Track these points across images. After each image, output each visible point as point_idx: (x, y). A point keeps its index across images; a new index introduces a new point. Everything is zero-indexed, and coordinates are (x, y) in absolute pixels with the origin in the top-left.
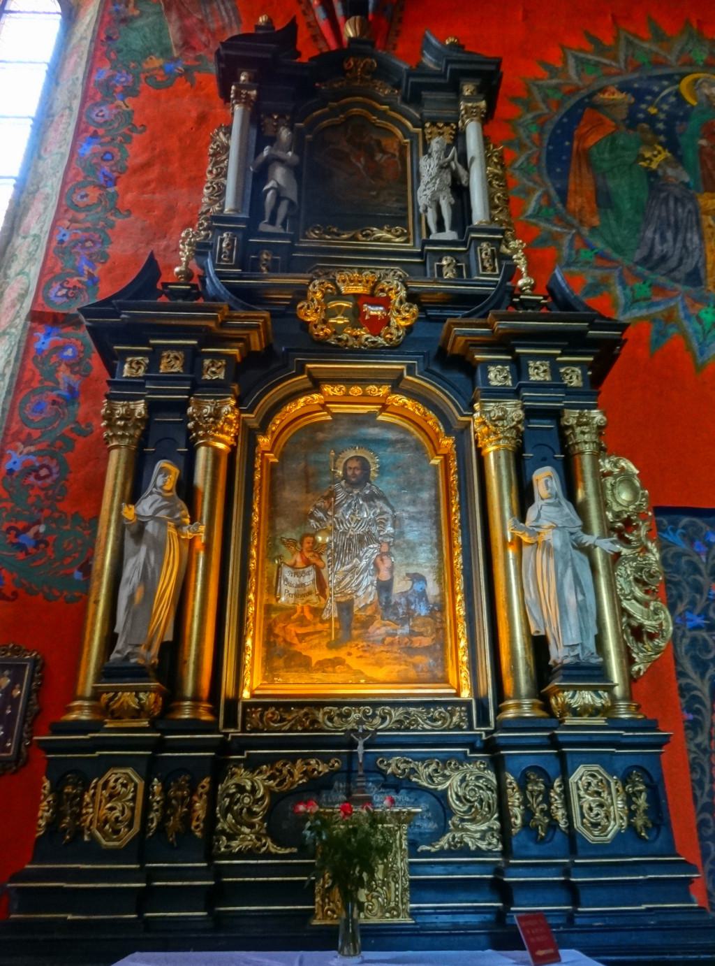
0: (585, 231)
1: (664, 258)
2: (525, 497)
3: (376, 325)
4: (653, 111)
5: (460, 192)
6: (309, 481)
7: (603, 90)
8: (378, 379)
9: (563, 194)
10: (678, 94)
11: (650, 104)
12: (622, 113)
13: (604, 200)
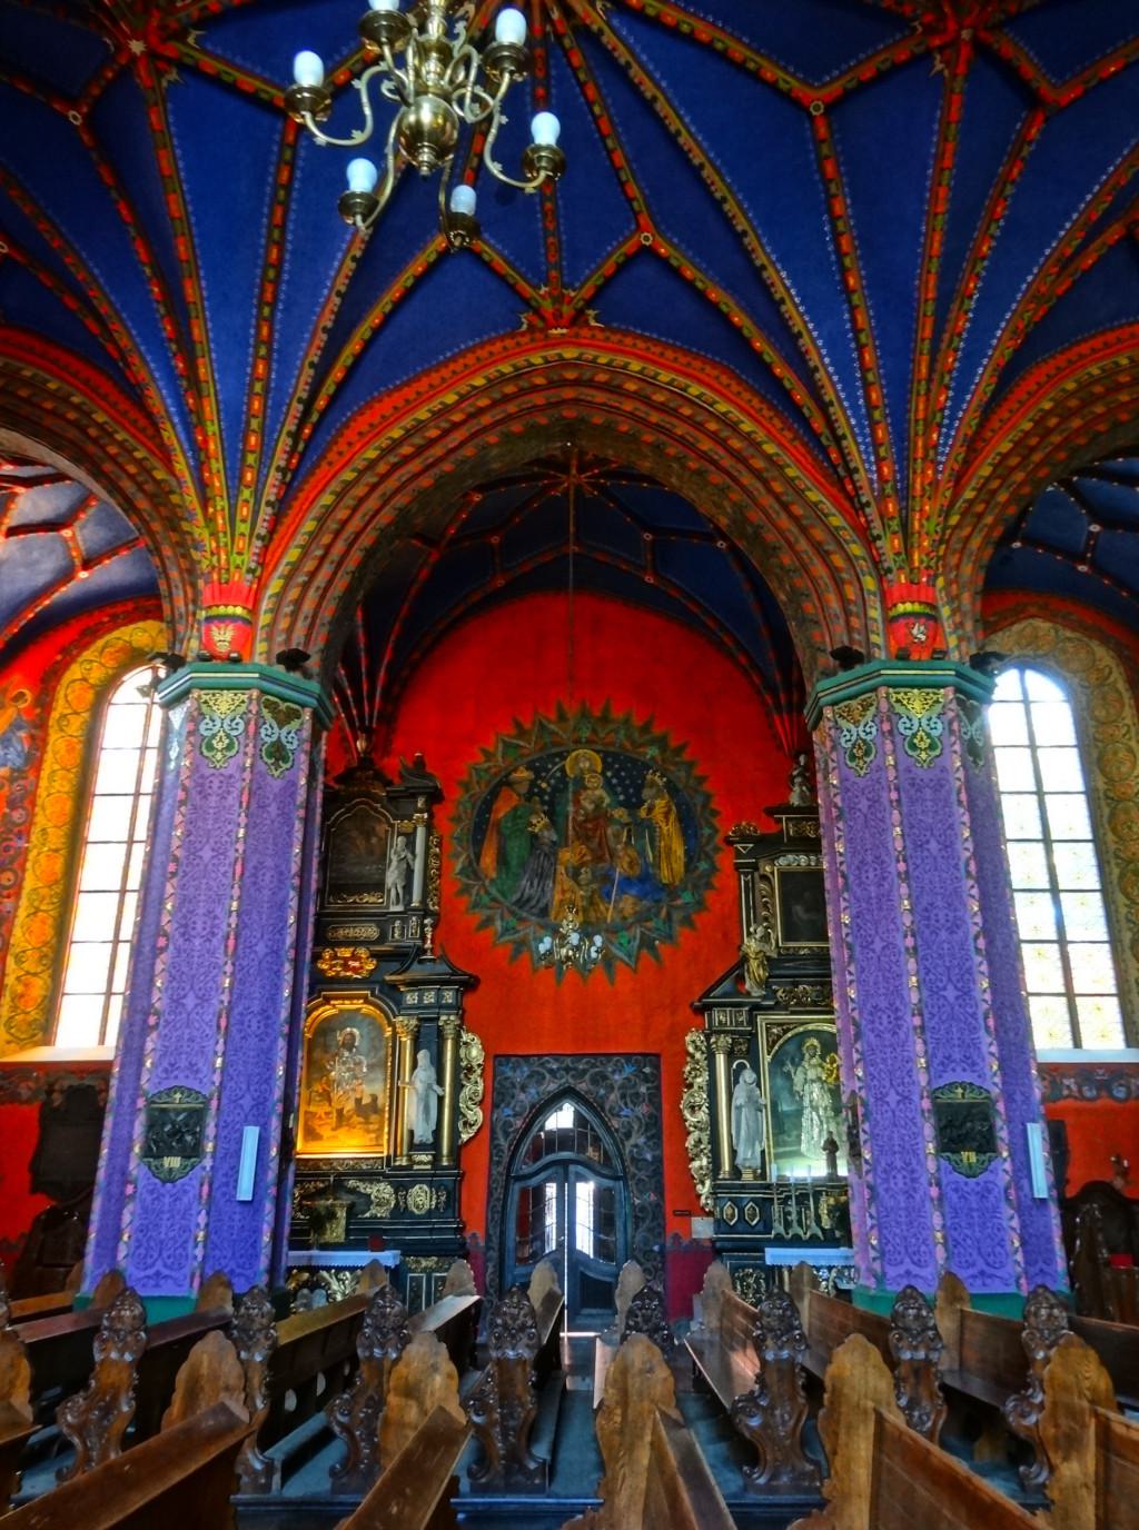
0: (487, 882)
1: (529, 900)
2: (414, 1065)
3: (355, 970)
4: (544, 785)
5: (409, 872)
6: (326, 1048)
7: (515, 770)
8: (358, 997)
9: (478, 857)
10: (563, 770)
11: (543, 779)
12: (523, 789)
13: (502, 860)
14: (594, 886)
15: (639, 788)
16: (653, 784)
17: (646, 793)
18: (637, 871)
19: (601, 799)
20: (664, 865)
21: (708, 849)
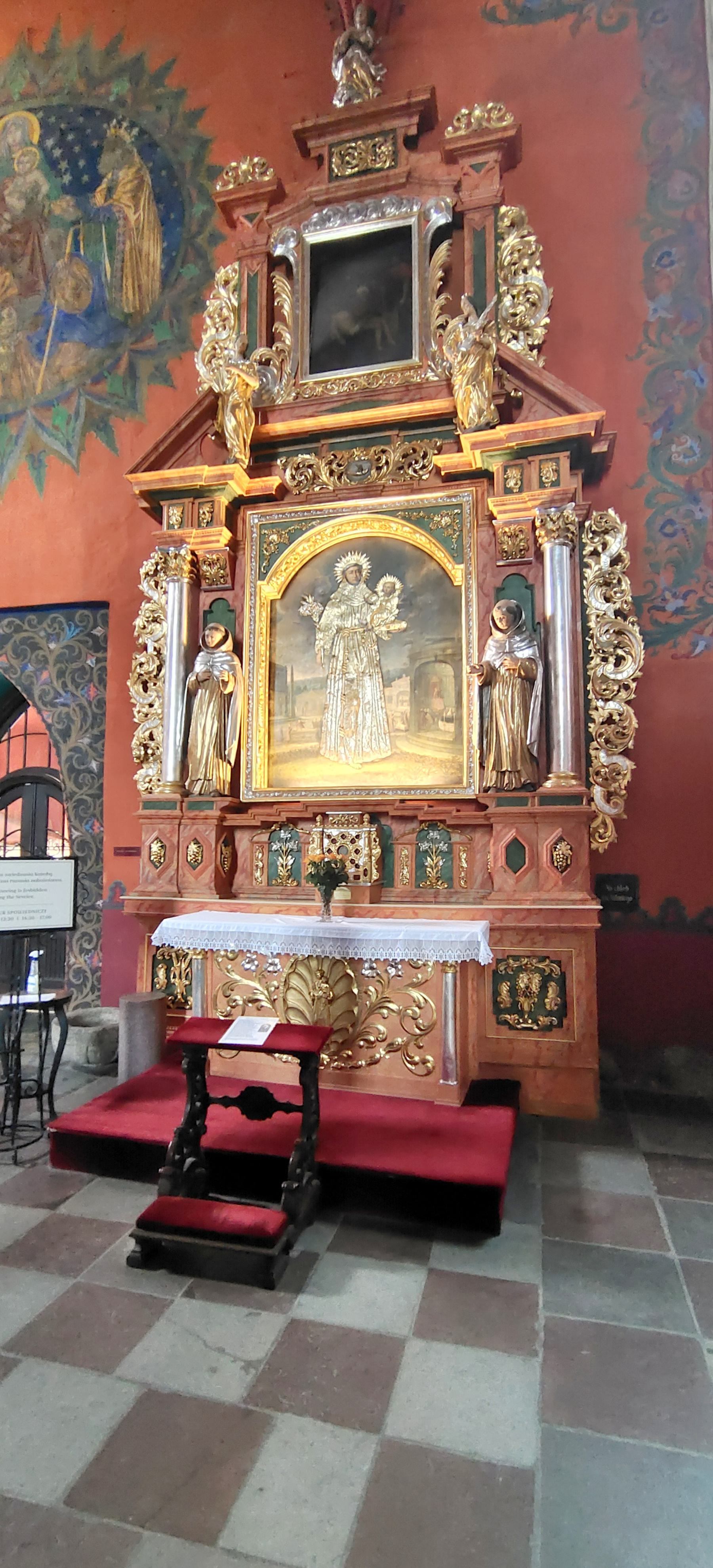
14: (20, 335)
15: (93, 156)
16: (118, 141)
17: (106, 161)
18: (86, 300)
19: (35, 188)
20: (128, 283)
21: (200, 240)
